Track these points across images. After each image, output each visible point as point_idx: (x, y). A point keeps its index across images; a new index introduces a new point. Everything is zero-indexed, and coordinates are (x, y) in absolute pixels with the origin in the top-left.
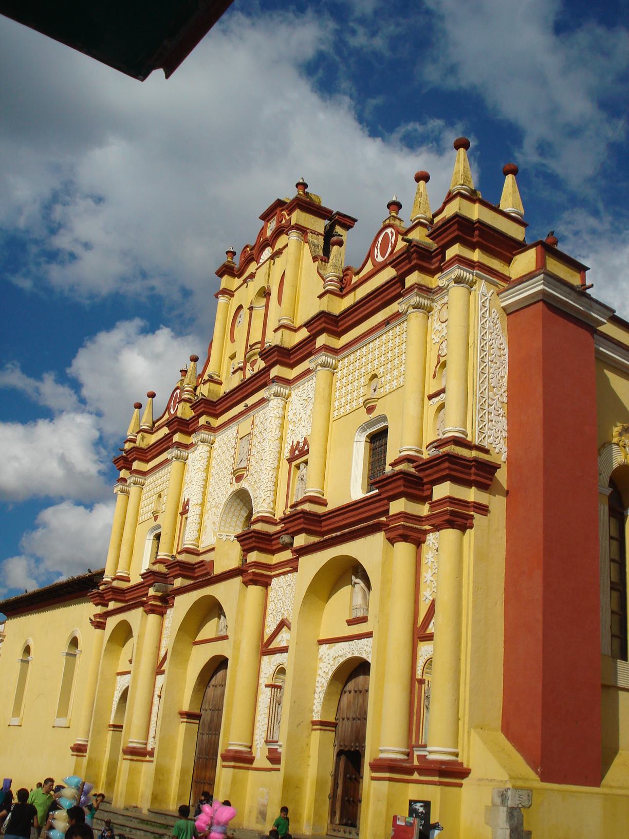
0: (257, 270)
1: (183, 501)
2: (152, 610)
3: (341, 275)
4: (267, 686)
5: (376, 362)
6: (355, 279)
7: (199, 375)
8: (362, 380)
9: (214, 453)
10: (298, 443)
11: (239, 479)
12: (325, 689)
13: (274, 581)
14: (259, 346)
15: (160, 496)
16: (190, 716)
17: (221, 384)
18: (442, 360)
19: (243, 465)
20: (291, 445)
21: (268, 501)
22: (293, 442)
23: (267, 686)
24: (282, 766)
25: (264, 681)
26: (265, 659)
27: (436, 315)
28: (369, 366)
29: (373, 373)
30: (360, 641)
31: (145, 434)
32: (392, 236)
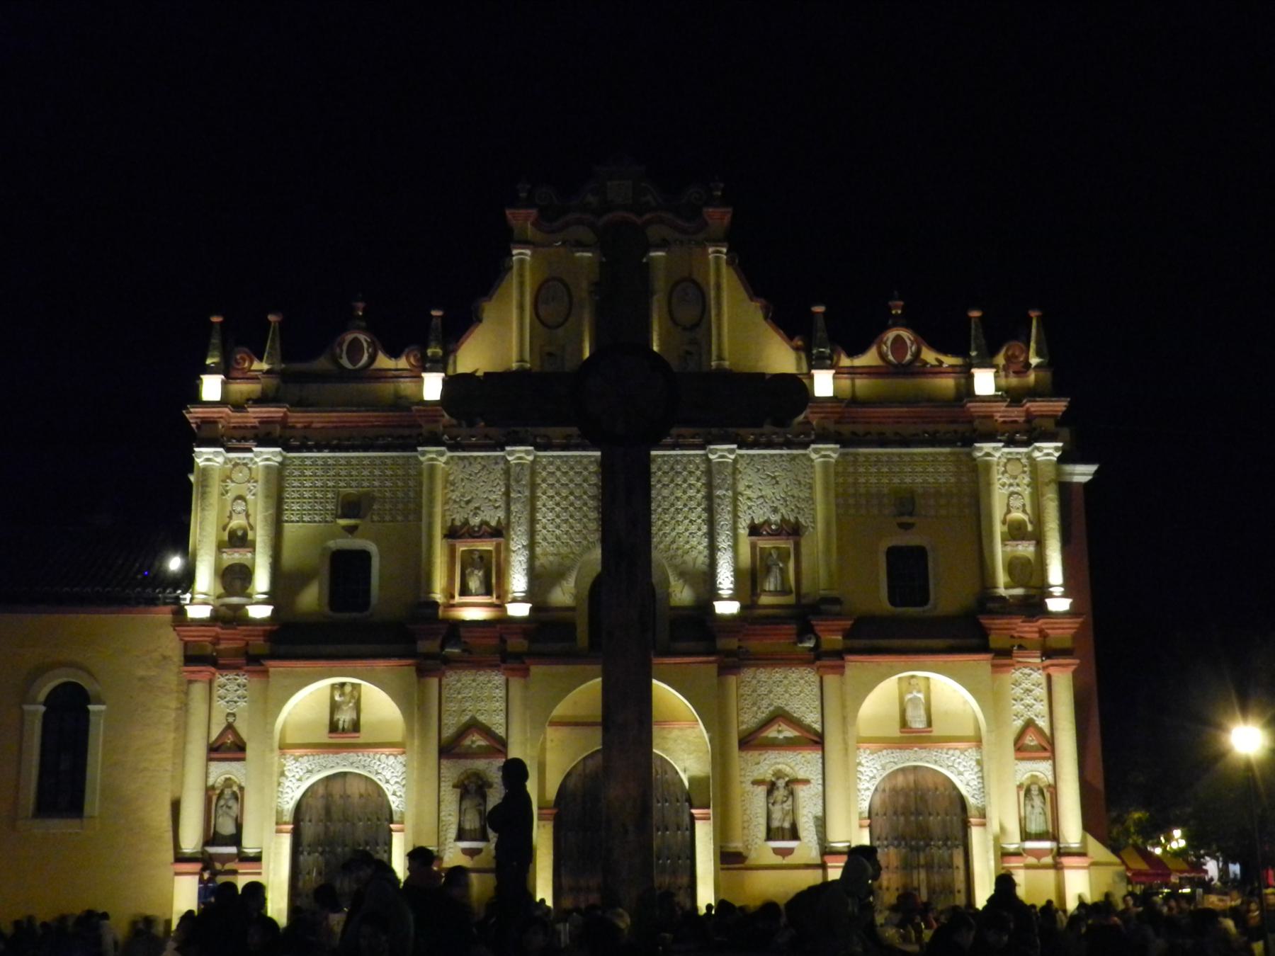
32: (912, 344)
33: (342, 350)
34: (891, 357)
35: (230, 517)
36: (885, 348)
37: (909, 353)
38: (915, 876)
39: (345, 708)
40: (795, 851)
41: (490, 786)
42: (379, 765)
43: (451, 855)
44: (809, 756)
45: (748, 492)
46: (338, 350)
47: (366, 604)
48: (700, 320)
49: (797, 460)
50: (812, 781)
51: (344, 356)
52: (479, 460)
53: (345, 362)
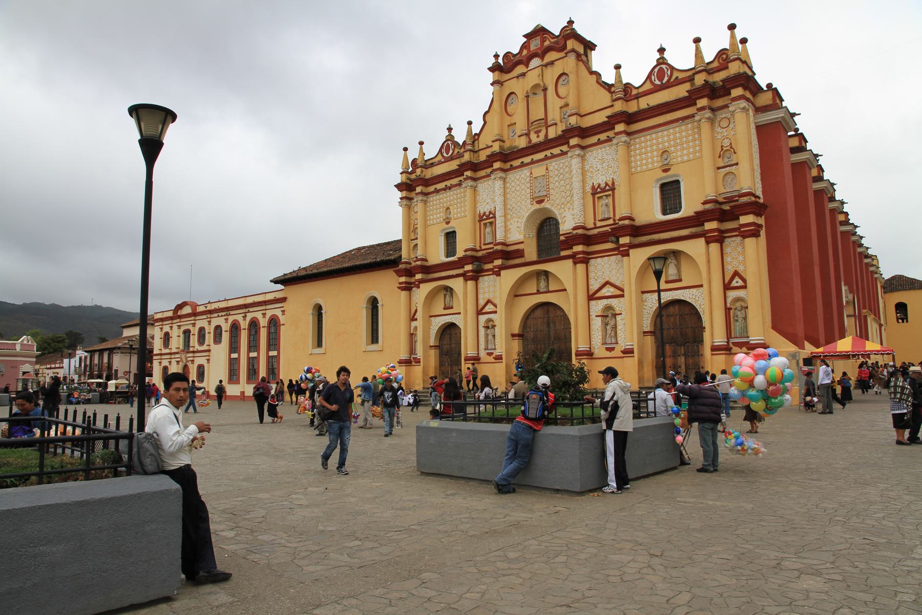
0: (528, 71)
1: (478, 213)
2: (472, 278)
3: (624, 88)
4: (596, 316)
5: (666, 144)
6: (634, 92)
7: (476, 134)
8: (655, 153)
9: (508, 185)
10: (599, 185)
13: (592, 262)
14: (543, 121)
15: (448, 208)
16: (519, 335)
17: (504, 142)
18: (725, 149)
19: (545, 194)
20: (592, 185)
21: (582, 217)
22: (593, 183)
23: (596, 316)
24: (422, 364)
25: (593, 314)
26: (593, 303)
27: (717, 125)
28: (661, 146)
29: (665, 150)
30: (677, 291)
31: (423, 169)
32: (668, 70)
34: (657, 82)
35: (414, 227)
36: (653, 78)
37: (666, 75)
38: (679, 360)
40: (616, 348)
47: (454, 254)
50: (623, 313)
53: (445, 155)
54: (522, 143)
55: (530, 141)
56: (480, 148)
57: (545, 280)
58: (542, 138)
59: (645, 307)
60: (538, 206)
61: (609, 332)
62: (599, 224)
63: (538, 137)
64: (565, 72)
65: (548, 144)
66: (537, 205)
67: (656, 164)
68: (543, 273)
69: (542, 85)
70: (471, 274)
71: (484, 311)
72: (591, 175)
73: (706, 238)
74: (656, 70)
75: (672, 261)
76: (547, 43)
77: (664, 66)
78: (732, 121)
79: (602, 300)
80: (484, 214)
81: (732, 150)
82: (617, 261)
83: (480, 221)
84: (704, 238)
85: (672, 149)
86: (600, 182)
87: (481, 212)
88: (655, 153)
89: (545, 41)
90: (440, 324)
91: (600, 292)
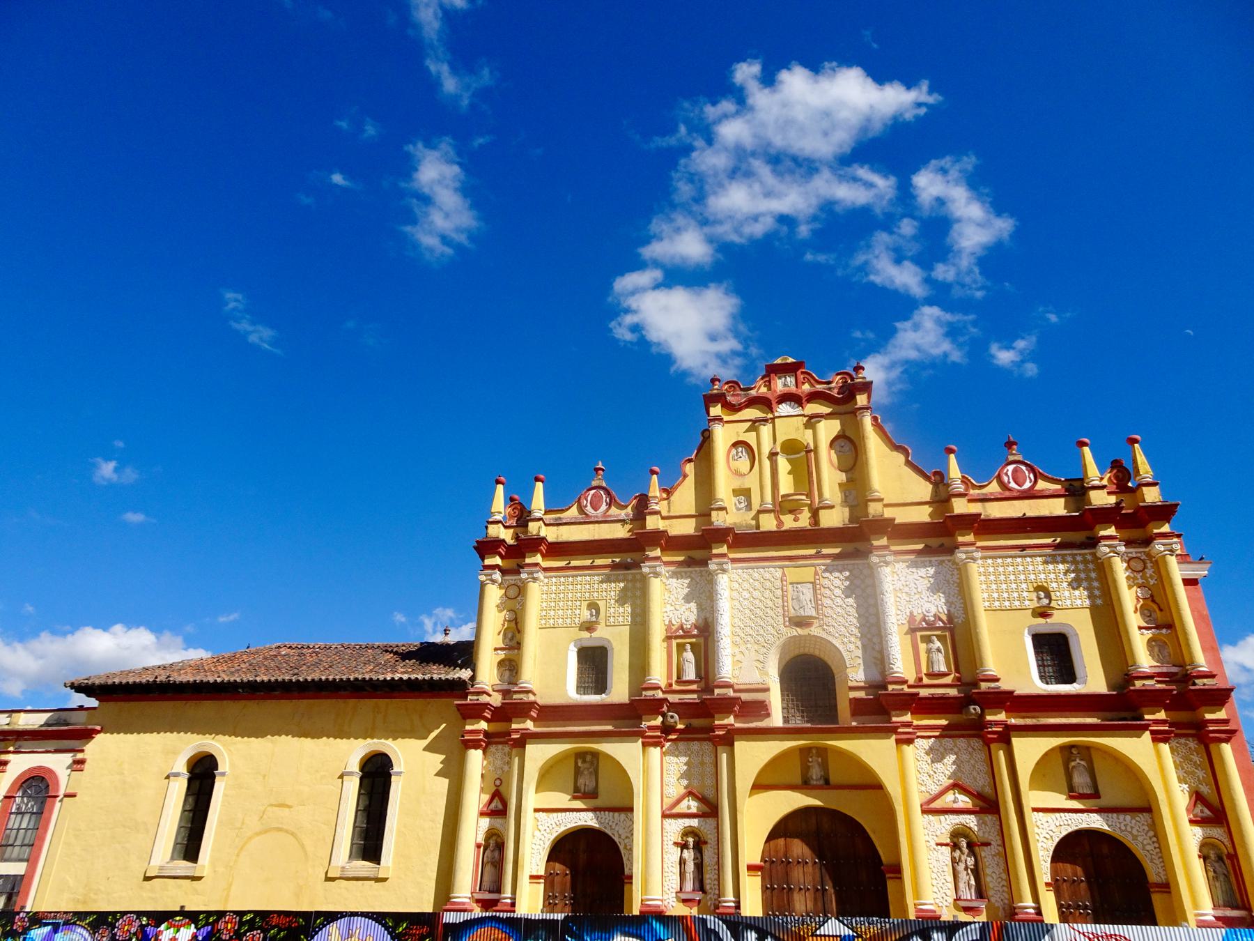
1: (667, 623)
4: (937, 844)
11: (809, 625)
12: (1051, 853)
19: (814, 614)
20: (908, 614)
22: (911, 613)
23: (937, 844)
32: (1029, 474)
33: (587, 501)
34: (1013, 485)
36: (1006, 479)
37: (1028, 480)
39: (586, 772)
41: (706, 843)
42: (613, 822)
43: (674, 904)
44: (986, 818)
45: (907, 589)
46: (585, 502)
48: (854, 465)
49: (944, 564)
50: (992, 842)
51: (589, 504)
52: (689, 573)
53: (589, 509)
54: (768, 523)
55: (780, 523)
56: (671, 514)
57: (819, 764)
58: (804, 521)
59: (1037, 837)
60: (800, 631)
61: (963, 876)
62: (926, 681)
63: (796, 520)
64: (848, 434)
65: (814, 537)
66: (798, 629)
67: (1027, 603)
68: (814, 751)
69: (806, 445)
70: (659, 734)
71: (676, 810)
72: (908, 599)
73: (1152, 732)
74: (1011, 468)
75: (1082, 763)
76: (806, 387)
77: (1024, 468)
78: (1149, 565)
79: (947, 816)
80: (682, 628)
81: (1155, 607)
82: (970, 749)
83: (669, 638)
84: (1148, 733)
85: (1054, 585)
86: (927, 614)
87: (674, 622)
88: (1024, 586)
89: (803, 383)
90: (562, 829)
91: (943, 797)
